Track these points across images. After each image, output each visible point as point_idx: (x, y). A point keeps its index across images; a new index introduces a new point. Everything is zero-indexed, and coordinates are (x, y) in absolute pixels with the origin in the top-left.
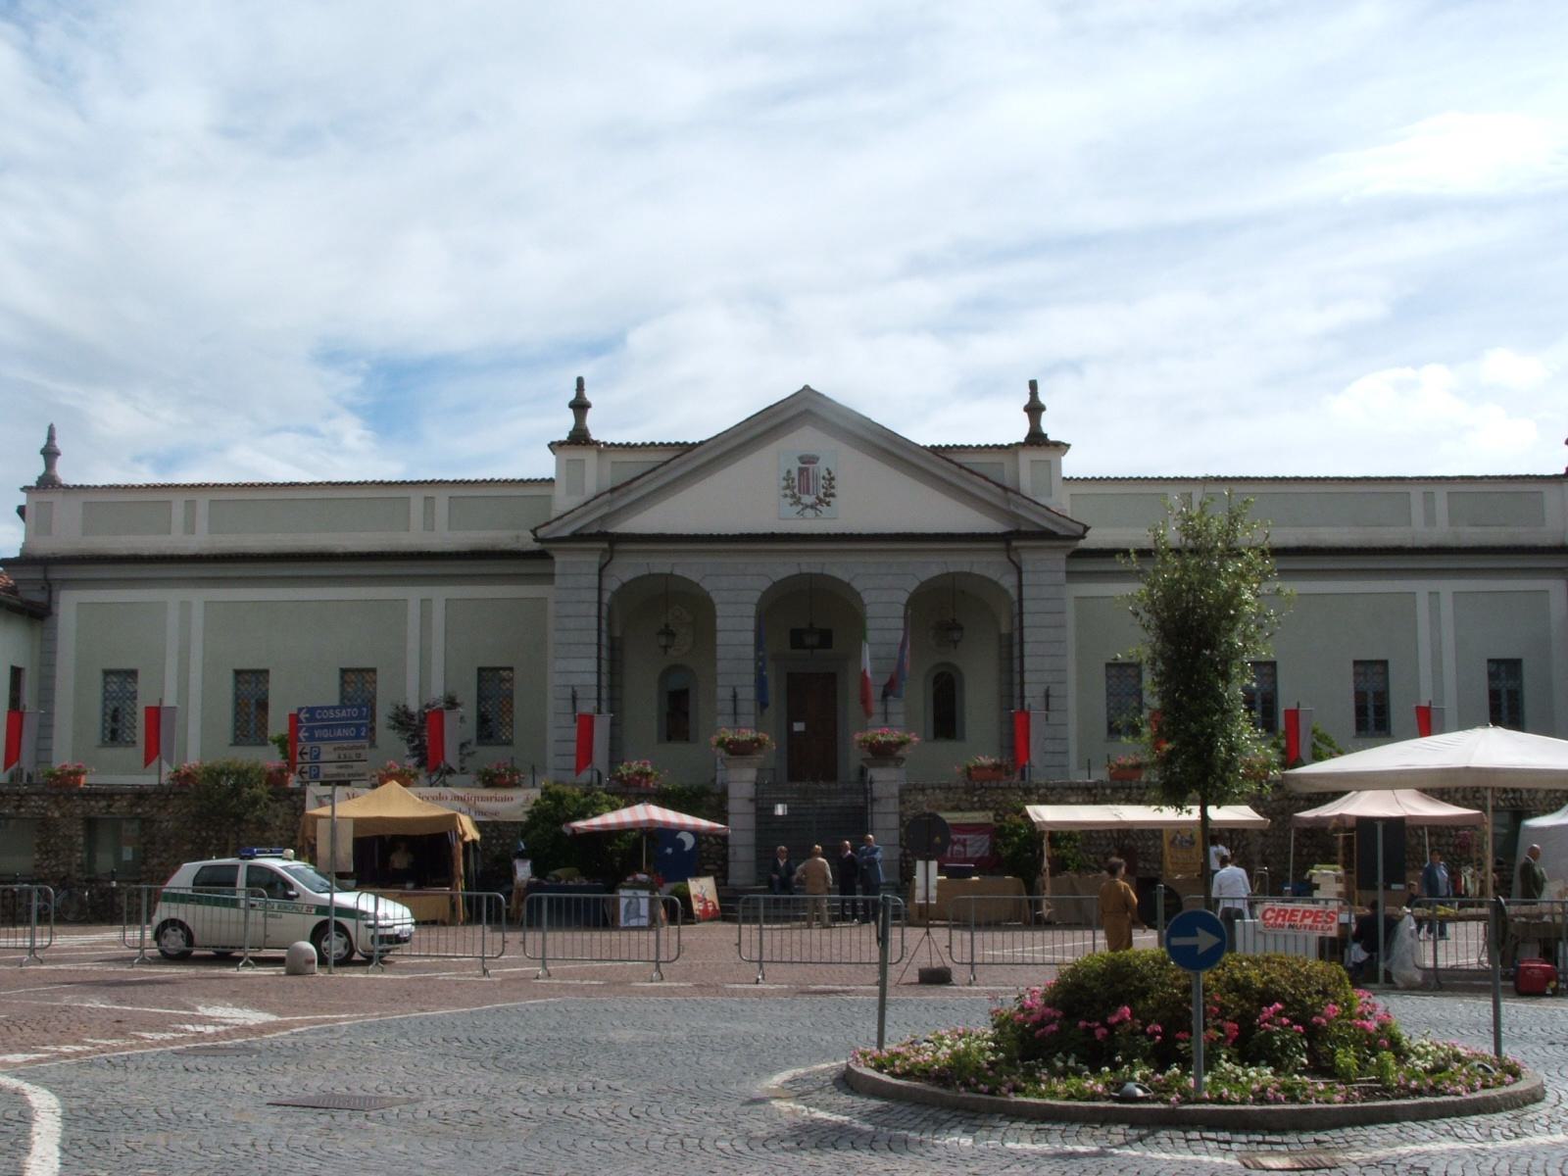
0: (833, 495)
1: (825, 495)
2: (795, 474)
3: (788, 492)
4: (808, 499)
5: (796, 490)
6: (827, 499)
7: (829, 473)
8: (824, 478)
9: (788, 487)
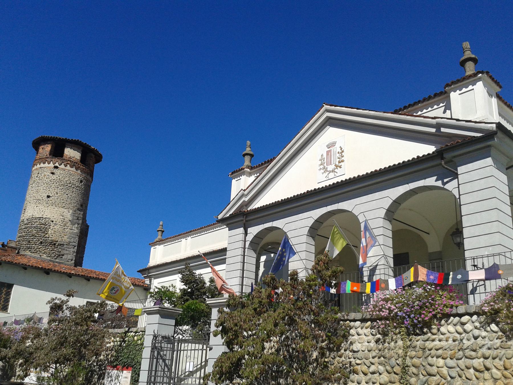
0: (343, 161)
1: (339, 162)
2: (325, 156)
3: (322, 167)
4: (331, 168)
5: (325, 165)
6: (340, 164)
7: (341, 149)
8: (338, 153)
9: (321, 164)
